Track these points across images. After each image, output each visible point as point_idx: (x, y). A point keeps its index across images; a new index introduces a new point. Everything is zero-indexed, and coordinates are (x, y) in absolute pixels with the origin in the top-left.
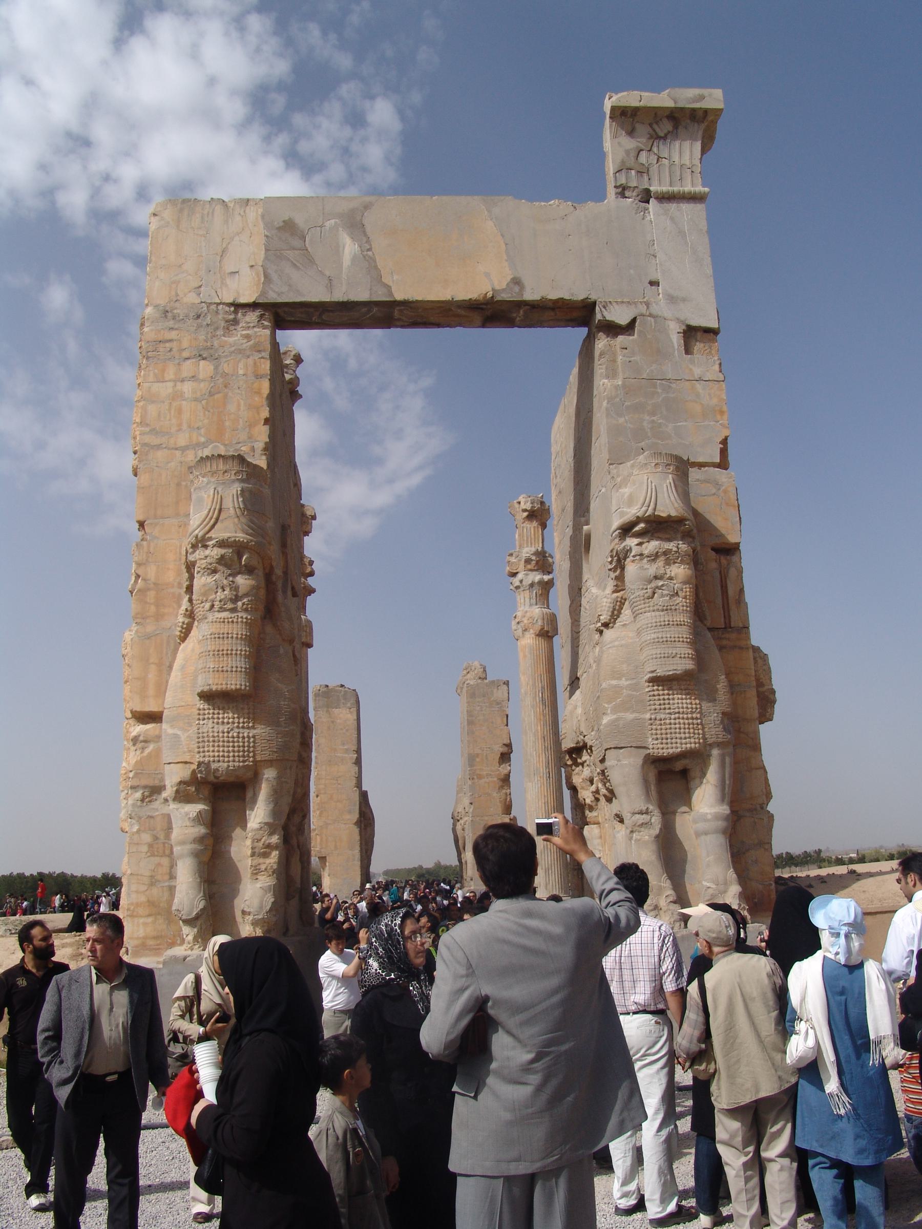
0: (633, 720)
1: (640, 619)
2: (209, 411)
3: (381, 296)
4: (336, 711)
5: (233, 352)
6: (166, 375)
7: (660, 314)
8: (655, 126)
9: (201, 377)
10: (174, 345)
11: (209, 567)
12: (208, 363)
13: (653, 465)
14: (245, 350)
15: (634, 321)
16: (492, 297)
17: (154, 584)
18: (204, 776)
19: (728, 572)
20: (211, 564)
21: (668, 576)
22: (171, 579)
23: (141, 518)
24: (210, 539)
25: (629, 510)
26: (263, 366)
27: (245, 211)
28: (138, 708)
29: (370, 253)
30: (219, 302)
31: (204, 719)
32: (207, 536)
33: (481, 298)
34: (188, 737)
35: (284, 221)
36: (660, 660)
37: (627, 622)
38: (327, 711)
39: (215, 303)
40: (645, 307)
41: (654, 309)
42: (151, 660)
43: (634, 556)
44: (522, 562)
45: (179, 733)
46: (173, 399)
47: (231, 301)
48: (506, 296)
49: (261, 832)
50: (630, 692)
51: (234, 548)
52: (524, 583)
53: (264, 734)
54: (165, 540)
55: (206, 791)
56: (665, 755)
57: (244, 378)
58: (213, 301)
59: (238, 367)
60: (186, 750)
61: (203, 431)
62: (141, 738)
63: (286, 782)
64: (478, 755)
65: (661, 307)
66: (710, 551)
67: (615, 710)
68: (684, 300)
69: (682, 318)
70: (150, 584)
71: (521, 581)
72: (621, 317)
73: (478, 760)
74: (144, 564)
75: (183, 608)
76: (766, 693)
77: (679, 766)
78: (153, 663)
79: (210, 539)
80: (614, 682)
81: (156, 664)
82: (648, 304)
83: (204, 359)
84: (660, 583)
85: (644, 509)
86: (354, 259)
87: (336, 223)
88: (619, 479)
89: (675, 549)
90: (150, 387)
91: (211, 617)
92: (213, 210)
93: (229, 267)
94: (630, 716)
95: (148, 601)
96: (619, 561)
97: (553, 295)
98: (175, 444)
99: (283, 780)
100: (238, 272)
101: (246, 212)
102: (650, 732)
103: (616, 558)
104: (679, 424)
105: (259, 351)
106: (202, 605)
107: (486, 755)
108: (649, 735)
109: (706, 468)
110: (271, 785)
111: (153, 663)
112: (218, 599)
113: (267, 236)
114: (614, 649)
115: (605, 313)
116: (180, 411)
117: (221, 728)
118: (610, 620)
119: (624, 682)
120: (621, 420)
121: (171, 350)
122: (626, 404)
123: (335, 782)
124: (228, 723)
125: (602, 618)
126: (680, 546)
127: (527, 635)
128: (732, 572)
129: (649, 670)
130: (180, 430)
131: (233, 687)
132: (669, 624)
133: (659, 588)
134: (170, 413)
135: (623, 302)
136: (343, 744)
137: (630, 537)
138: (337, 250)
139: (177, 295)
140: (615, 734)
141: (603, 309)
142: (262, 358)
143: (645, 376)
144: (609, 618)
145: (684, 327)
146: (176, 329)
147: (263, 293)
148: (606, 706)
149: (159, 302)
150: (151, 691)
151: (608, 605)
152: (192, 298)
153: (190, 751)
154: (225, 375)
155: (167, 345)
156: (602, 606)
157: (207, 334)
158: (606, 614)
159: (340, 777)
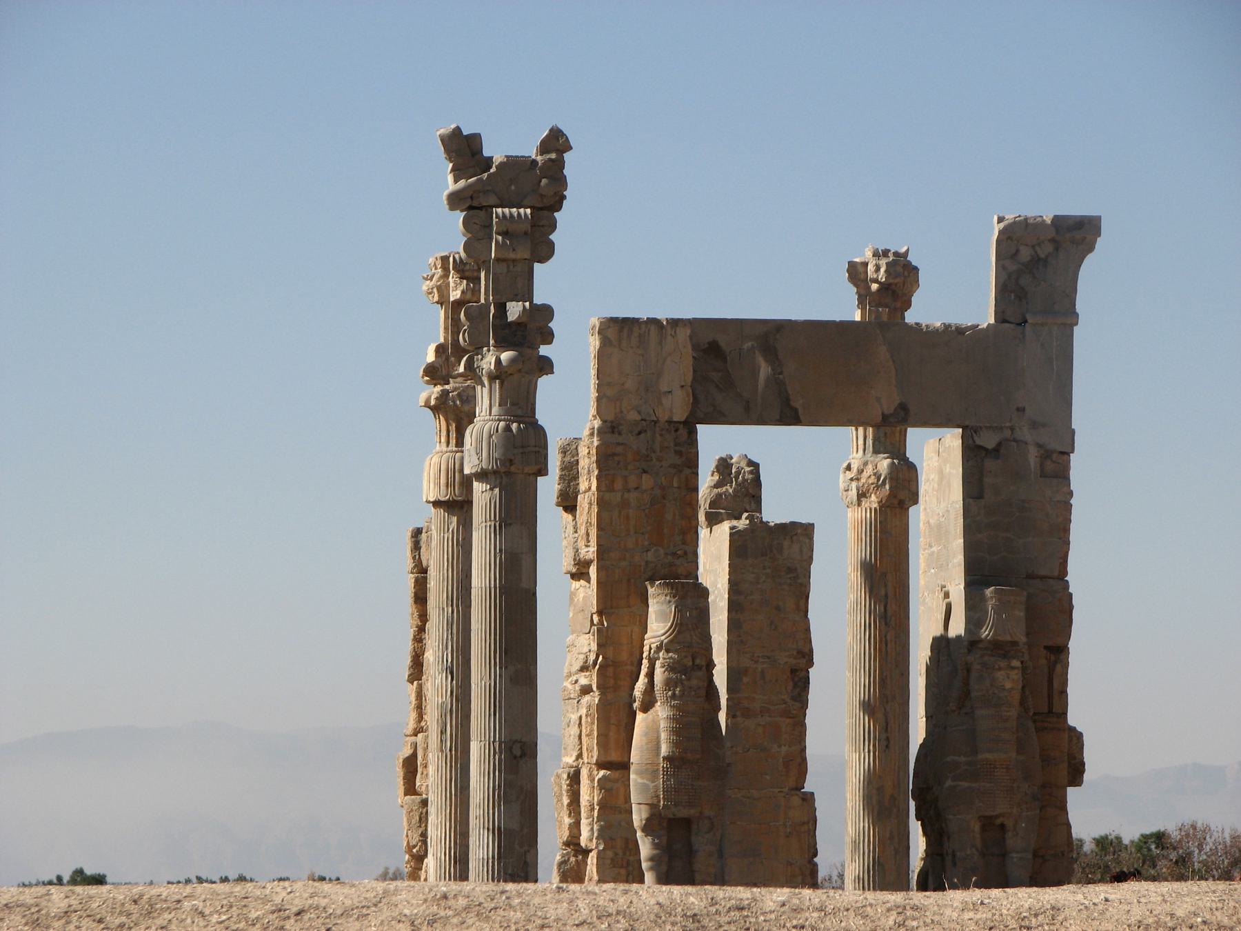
5: (669, 467)
6: (615, 486)
8: (1038, 249)
9: (644, 488)
12: (649, 476)
15: (999, 444)
27: (675, 332)
28: (603, 759)
29: (781, 376)
35: (708, 343)
39: (653, 421)
47: (666, 418)
61: (647, 536)
64: (746, 671)
65: (1026, 434)
66: (1042, 649)
68: (1044, 425)
73: (745, 680)
77: (998, 822)
82: (1012, 429)
83: (645, 472)
86: (767, 380)
87: (752, 345)
92: (649, 331)
93: (664, 387)
100: (669, 392)
101: (677, 332)
105: (689, 467)
107: (763, 672)
113: (693, 357)
116: (628, 518)
119: (963, 759)
121: (618, 464)
128: (1059, 667)
135: (990, 427)
138: (755, 372)
139: (622, 412)
152: (633, 416)
155: (616, 458)
157: (647, 449)
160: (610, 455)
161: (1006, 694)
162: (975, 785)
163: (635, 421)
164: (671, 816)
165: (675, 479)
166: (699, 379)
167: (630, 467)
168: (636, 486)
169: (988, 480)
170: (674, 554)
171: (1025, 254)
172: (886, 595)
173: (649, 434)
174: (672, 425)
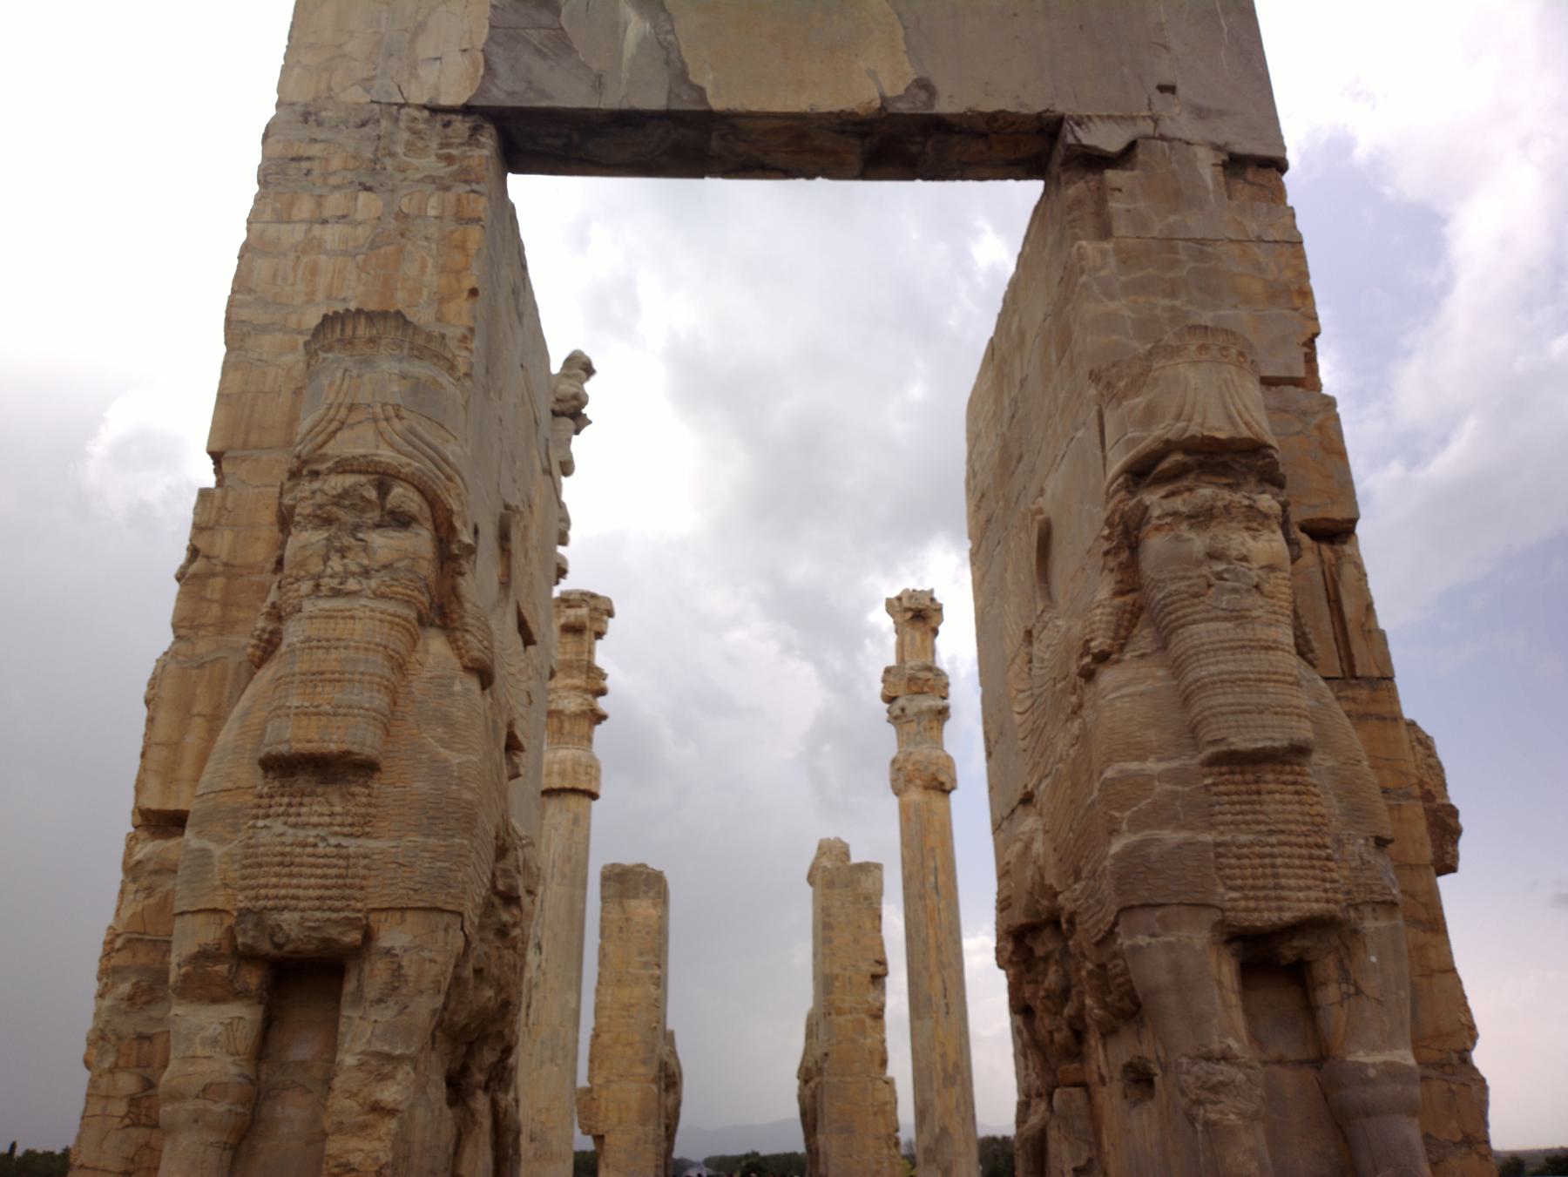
0: (1179, 846)
1: (1181, 637)
2: (368, 274)
3: (685, 103)
5: (421, 180)
7: (1178, 135)
9: (359, 216)
10: (316, 166)
11: (319, 512)
12: (373, 196)
13: (1193, 348)
14: (442, 178)
15: (1131, 147)
16: (883, 108)
17: (226, 565)
18: (249, 942)
19: (1339, 575)
20: (320, 507)
21: (1234, 553)
22: (260, 558)
23: (216, 448)
24: (323, 458)
25: (1144, 434)
26: (473, 205)
30: (402, 101)
31: (267, 816)
32: (319, 452)
33: (860, 111)
34: (226, 854)
36: (1231, 717)
37: (1149, 651)
39: (395, 104)
40: (1152, 124)
41: (1168, 129)
42: (196, 710)
43: (1159, 518)
44: (904, 683)
45: (212, 846)
46: (304, 252)
47: (424, 100)
48: (903, 107)
49: (362, 1075)
50: (1168, 787)
51: (372, 477)
52: (908, 712)
53: (394, 850)
54: (257, 487)
55: (252, 978)
56: (1258, 924)
57: (436, 222)
58: (393, 101)
59: (426, 204)
60: (218, 883)
62: (151, 866)
63: (432, 961)
67: (1135, 825)
69: (1220, 141)
70: (215, 565)
71: (903, 710)
72: (1109, 139)
74: (211, 529)
75: (270, 600)
76: (1439, 814)
78: (199, 715)
79: (323, 458)
80: (1134, 766)
81: (204, 716)
82: (1156, 120)
83: (368, 189)
84: (1220, 567)
85: (1181, 424)
88: (1122, 384)
89: (1247, 502)
90: (264, 231)
91: (309, 607)
94: (1172, 836)
95: (208, 595)
96: (1126, 532)
97: (989, 106)
98: (299, 322)
99: (426, 954)
102: (1221, 873)
103: (1120, 527)
104: (1222, 313)
105: (467, 182)
106: (295, 586)
108: (1218, 881)
109: (1282, 387)
110: (395, 966)
111: (199, 715)
112: (329, 571)
114: (1126, 699)
115: (1080, 134)
116: (314, 271)
117: (301, 834)
118: (1111, 646)
119: (1152, 766)
120: (1113, 305)
121: (308, 173)
122: (1123, 278)
124: (316, 826)
125: (1093, 644)
126: (1256, 497)
127: (912, 788)
128: (1348, 571)
129: (1208, 738)
130: (307, 302)
131: (333, 747)
132: (1243, 647)
133: (1219, 576)
134: (295, 275)
135: (1109, 117)
137: (1150, 485)
140: (1142, 876)
141: (1076, 128)
142: (473, 192)
143: (1155, 234)
144: (1109, 641)
145: (1225, 157)
146: (322, 141)
148: (1117, 814)
149: (294, 99)
151: (1105, 618)
153: (226, 886)
154: (402, 216)
155: (305, 165)
156: (1094, 623)
158: (1104, 636)
160: (293, 159)
161: (1256, 580)
162: (1209, 837)
163: (358, 104)
164: (266, 947)
165: (433, 202)
168: (340, 213)
169: (1116, 205)
172: (936, 868)
173: (385, 124)
174: (439, 117)
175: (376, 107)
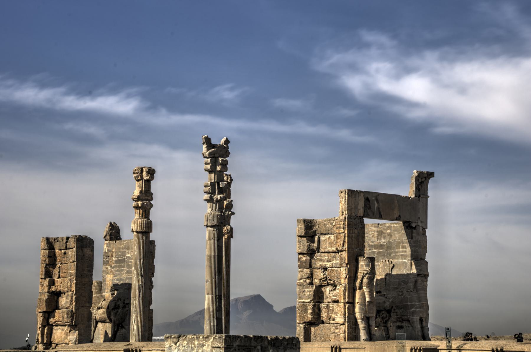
4: (85, 250)
9: (356, 233)
15: (416, 226)
38: (82, 250)
47: (359, 216)
72: (414, 225)
83: (356, 229)
93: (359, 208)
116: (353, 240)
119: (417, 303)
123: (83, 286)
136: (88, 267)
147: (364, 215)
150: (350, 298)
152: (354, 215)
159: (85, 284)
162: (420, 310)
166: (365, 206)
167: (353, 227)
170: (361, 250)
171: (420, 180)
173: (356, 219)
175: (356, 217)
